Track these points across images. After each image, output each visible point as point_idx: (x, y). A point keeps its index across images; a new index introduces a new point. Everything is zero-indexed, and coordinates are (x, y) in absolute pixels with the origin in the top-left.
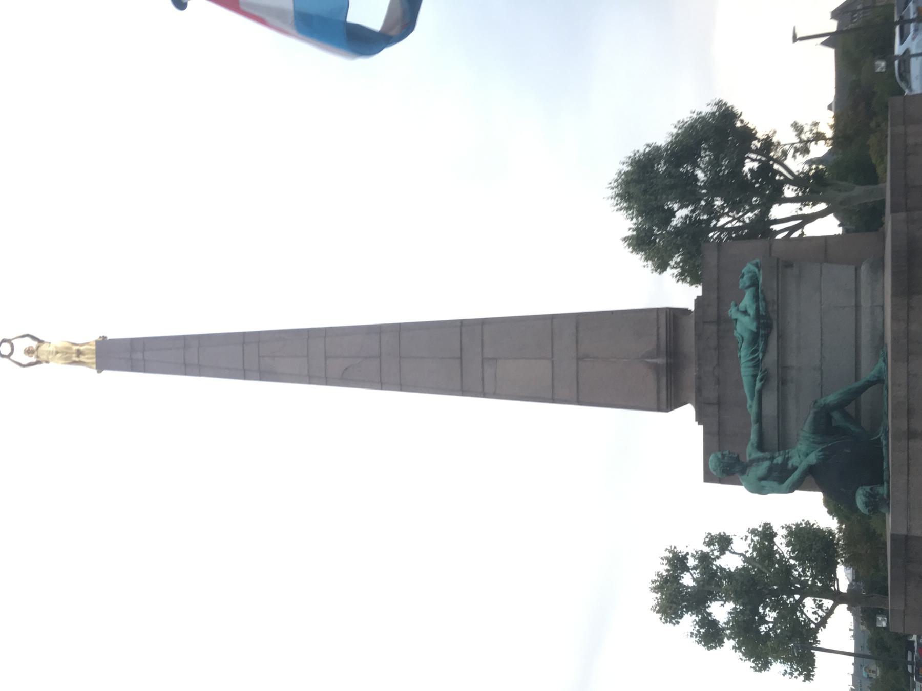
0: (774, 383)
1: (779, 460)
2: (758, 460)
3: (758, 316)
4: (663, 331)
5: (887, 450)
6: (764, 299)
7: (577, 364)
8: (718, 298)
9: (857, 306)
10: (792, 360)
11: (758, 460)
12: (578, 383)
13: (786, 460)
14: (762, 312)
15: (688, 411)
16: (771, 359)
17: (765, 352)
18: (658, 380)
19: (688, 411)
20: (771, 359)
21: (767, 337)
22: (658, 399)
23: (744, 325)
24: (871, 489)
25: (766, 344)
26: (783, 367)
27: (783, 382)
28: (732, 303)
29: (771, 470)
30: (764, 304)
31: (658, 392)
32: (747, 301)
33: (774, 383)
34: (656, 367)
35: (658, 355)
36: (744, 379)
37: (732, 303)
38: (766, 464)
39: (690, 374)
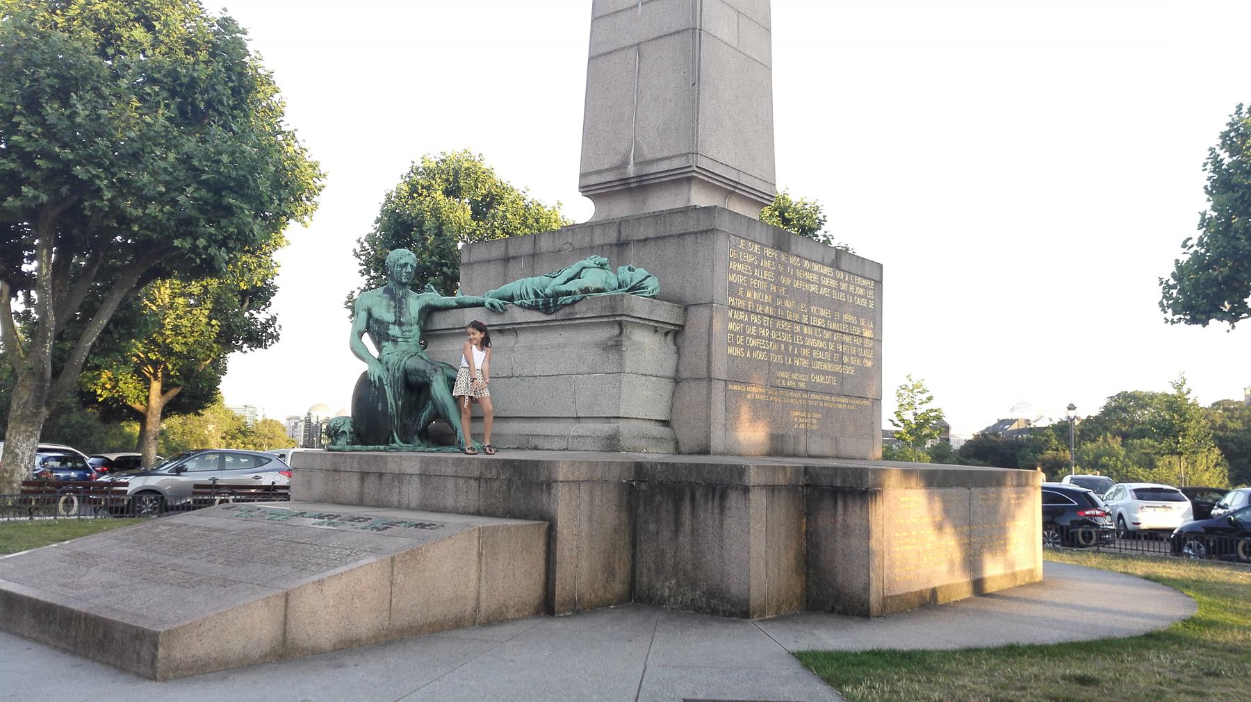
3: (557, 295)
4: (665, 166)
5: (385, 450)
6: (574, 302)
7: (631, 46)
8: (646, 240)
12: (610, 53)
13: (395, 341)
14: (561, 300)
16: (518, 315)
17: (521, 306)
20: (518, 315)
22: (590, 174)
24: (344, 432)
25: (530, 308)
28: (605, 260)
29: (380, 322)
30: (570, 301)
31: (599, 172)
34: (624, 164)
36: (519, 282)
37: (605, 260)
38: (389, 317)
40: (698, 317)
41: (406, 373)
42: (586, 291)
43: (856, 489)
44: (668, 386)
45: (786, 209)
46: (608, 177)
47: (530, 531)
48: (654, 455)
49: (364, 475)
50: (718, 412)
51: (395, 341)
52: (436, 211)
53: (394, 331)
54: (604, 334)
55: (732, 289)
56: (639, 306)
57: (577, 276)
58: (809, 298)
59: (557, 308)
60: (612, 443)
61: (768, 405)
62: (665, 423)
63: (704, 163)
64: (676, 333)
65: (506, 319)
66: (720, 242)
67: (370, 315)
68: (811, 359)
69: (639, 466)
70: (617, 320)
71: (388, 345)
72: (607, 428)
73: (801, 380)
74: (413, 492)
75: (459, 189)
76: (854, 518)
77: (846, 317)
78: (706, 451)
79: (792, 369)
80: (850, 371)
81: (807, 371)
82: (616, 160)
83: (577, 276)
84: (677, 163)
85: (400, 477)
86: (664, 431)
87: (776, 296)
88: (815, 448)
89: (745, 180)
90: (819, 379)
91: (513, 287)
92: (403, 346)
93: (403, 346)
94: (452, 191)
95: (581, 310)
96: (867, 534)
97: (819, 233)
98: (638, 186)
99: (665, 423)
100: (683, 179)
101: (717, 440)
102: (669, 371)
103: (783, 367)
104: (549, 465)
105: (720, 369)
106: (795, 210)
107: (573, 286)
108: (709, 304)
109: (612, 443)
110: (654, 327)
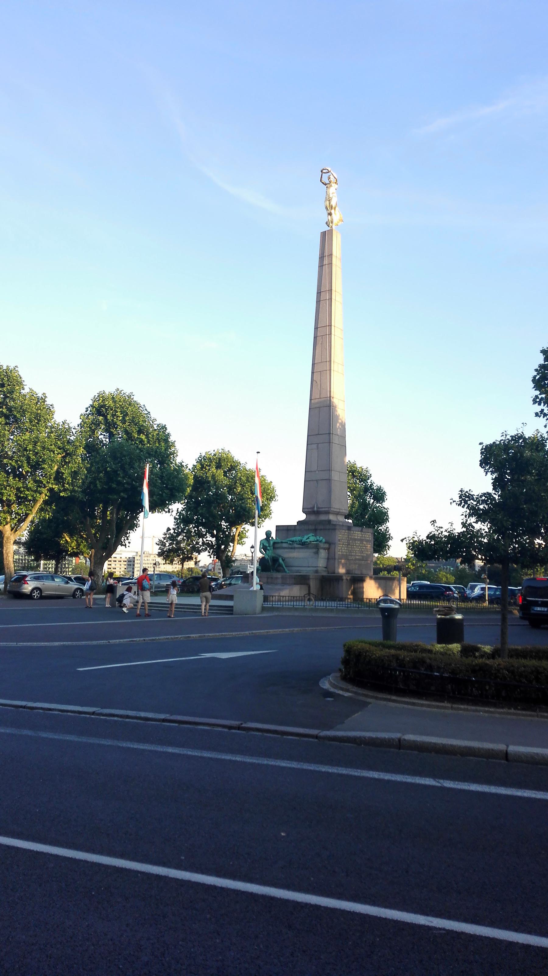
0: (290, 546)
1: (268, 548)
2: (269, 543)
3: (305, 542)
4: (323, 509)
9: (309, 567)
10: (296, 550)
11: (269, 543)
13: (269, 550)
15: (303, 517)
18: (310, 508)
19: (303, 517)
21: (300, 544)
23: (304, 539)
26: (294, 548)
27: (291, 548)
31: (307, 509)
32: (312, 539)
33: (290, 546)
34: (314, 507)
35: (318, 508)
38: (267, 545)
39: (313, 518)
40: (333, 546)
41: (273, 557)
42: (311, 542)
43: (361, 580)
44: (326, 561)
45: (355, 471)
46: (310, 510)
47: (305, 587)
48: (325, 574)
49: (268, 578)
50: (336, 565)
51: (269, 550)
52: (213, 476)
53: (268, 548)
54: (314, 550)
55: (339, 540)
56: (322, 545)
57: (308, 538)
58: (355, 540)
59: (305, 545)
60: (317, 572)
61: (346, 564)
62: (326, 568)
63: (332, 509)
64: (328, 549)
65: (293, 546)
66: (337, 531)
67: (263, 544)
68: (356, 553)
69: (323, 576)
70: (317, 548)
71: (267, 551)
72: (315, 569)
73: (353, 558)
74: (280, 581)
75: (221, 466)
76: (361, 585)
77: (364, 543)
78: (334, 573)
79: (352, 555)
80: (365, 555)
81: (355, 556)
82: (312, 506)
83: (308, 538)
84: (326, 509)
85: (277, 578)
86: (326, 569)
87: (348, 540)
88: (356, 572)
89: (341, 511)
90: (358, 557)
91: (294, 539)
92: (270, 551)
93: (270, 551)
94: (218, 467)
95: (310, 546)
96: (363, 588)
97: (369, 481)
98: (318, 513)
99: (326, 568)
100: (327, 513)
101: (336, 571)
102: (326, 557)
103: (350, 555)
104: (309, 575)
105: (337, 557)
106: (358, 471)
107: (308, 540)
108: (335, 544)
109: (317, 572)
110: (324, 549)
